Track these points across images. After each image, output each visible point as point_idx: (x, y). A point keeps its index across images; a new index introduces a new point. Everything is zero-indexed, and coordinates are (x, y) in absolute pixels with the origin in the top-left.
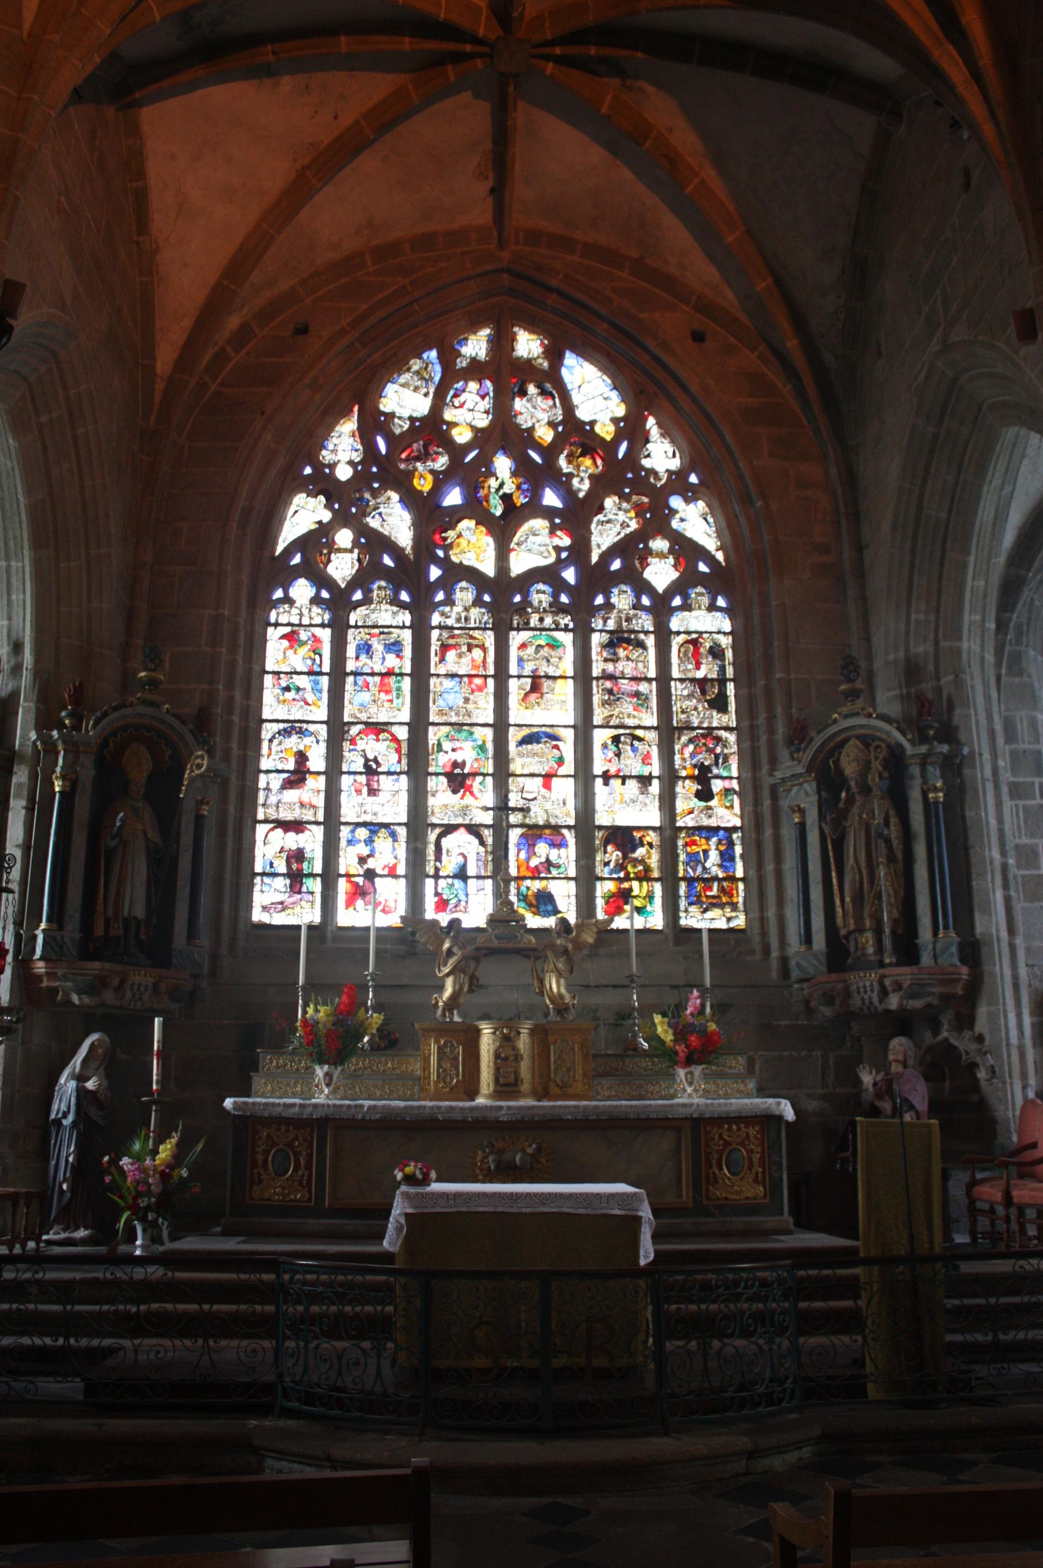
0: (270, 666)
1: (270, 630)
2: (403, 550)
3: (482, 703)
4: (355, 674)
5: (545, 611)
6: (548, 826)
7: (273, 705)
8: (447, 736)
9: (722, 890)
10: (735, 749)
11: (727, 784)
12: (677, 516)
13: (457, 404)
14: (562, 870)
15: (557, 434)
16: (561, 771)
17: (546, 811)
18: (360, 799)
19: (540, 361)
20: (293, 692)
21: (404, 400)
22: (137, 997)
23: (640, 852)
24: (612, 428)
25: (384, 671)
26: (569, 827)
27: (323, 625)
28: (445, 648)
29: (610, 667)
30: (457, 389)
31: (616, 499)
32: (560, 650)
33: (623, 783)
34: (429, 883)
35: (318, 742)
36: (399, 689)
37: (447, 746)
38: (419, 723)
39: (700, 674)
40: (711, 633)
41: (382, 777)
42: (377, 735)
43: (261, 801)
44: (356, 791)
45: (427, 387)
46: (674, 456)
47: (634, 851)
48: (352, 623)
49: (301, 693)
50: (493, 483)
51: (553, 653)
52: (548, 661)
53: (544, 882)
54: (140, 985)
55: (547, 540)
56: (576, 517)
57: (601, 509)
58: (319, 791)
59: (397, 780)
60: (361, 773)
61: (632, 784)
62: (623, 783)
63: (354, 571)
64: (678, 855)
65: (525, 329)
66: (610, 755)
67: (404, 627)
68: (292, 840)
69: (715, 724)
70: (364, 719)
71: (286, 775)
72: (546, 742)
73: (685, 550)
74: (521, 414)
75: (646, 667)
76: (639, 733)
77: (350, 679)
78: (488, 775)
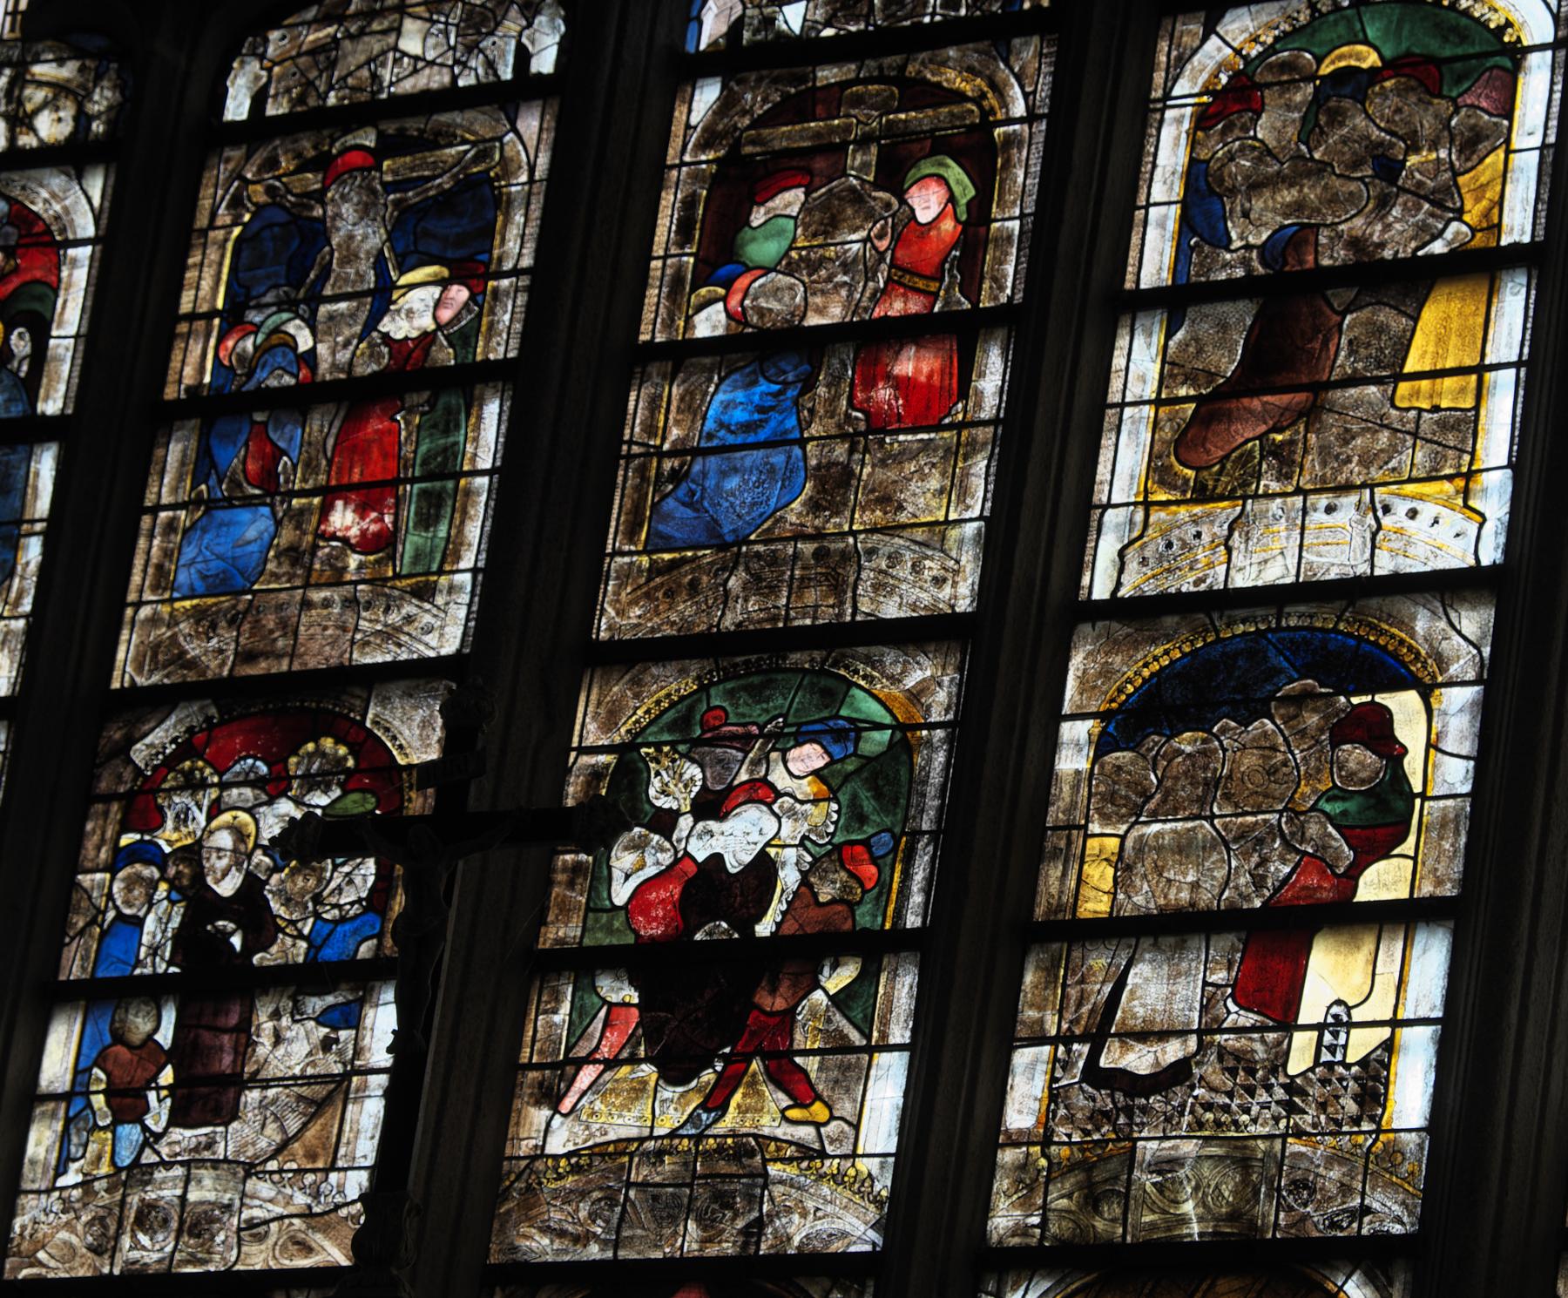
3: (923, 497)
4: (217, 407)
8: (681, 724)
16: (1383, 882)
17: (1240, 1157)
25: (365, 369)
36: (446, 469)
37: (675, 784)
48: (237, 107)
59: (349, 1016)
60: (153, 991)
72: (1301, 700)
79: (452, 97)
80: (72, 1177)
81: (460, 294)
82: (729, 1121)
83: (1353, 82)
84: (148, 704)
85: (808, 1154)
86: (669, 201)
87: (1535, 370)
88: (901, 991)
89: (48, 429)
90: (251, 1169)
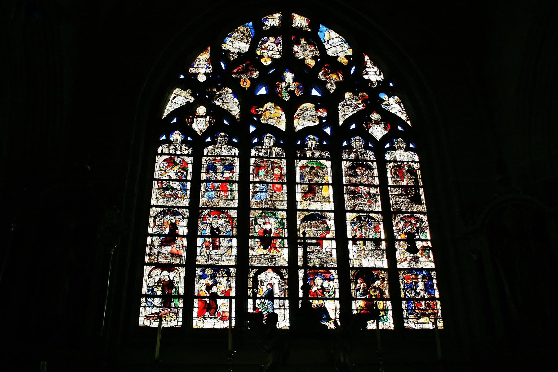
0: (156, 176)
1: (158, 157)
2: (234, 117)
3: (280, 198)
4: (206, 181)
5: (315, 149)
6: (321, 267)
7: (157, 198)
8: (260, 216)
9: (428, 305)
10: (427, 224)
11: (425, 244)
12: (384, 103)
13: (263, 47)
14: (331, 294)
15: (317, 63)
16: (328, 236)
18: (208, 251)
19: (307, 29)
20: (169, 191)
21: (236, 44)
23: (378, 283)
24: (346, 61)
26: (334, 269)
27: (188, 155)
28: (258, 168)
29: (353, 180)
30: (263, 40)
31: (351, 94)
32: (324, 170)
33: (365, 243)
34: (250, 302)
35: (183, 218)
36: (232, 191)
37: (260, 221)
38: (244, 208)
39: (404, 183)
40: (408, 162)
41: (221, 239)
42: (219, 215)
43: (148, 251)
44: (205, 247)
45: (247, 39)
46: (380, 74)
47: (374, 283)
48: (205, 153)
50: (283, 84)
51: (320, 171)
52: (318, 176)
53: (321, 301)
55: (314, 114)
56: (329, 102)
57: (344, 98)
58: (183, 247)
59: (231, 240)
60: (209, 237)
61: (369, 243)
62: (365, 243)
63: (207, 127)
64: (399, 285)
65: (299, 14)
66: (356, 227)
67: (234, 156)
69: (415, 210)
70: (211, 206)
71: (163, 238)
73: (389, 119)
74: (298, 53)
75: (373, 179)
76: (372, 215)
77: (203, 184)
78: (285, 238)
79: (227, 156)
80: (202, 254)
81: (231, 174)
82: (270, 254)
83: (314, 168)
84: (203, 209)
85: (279, 257)
86: (252, 168)
87: (334, 193)
88: (286, 241)
89: (189, 181)
90: (222, 255)
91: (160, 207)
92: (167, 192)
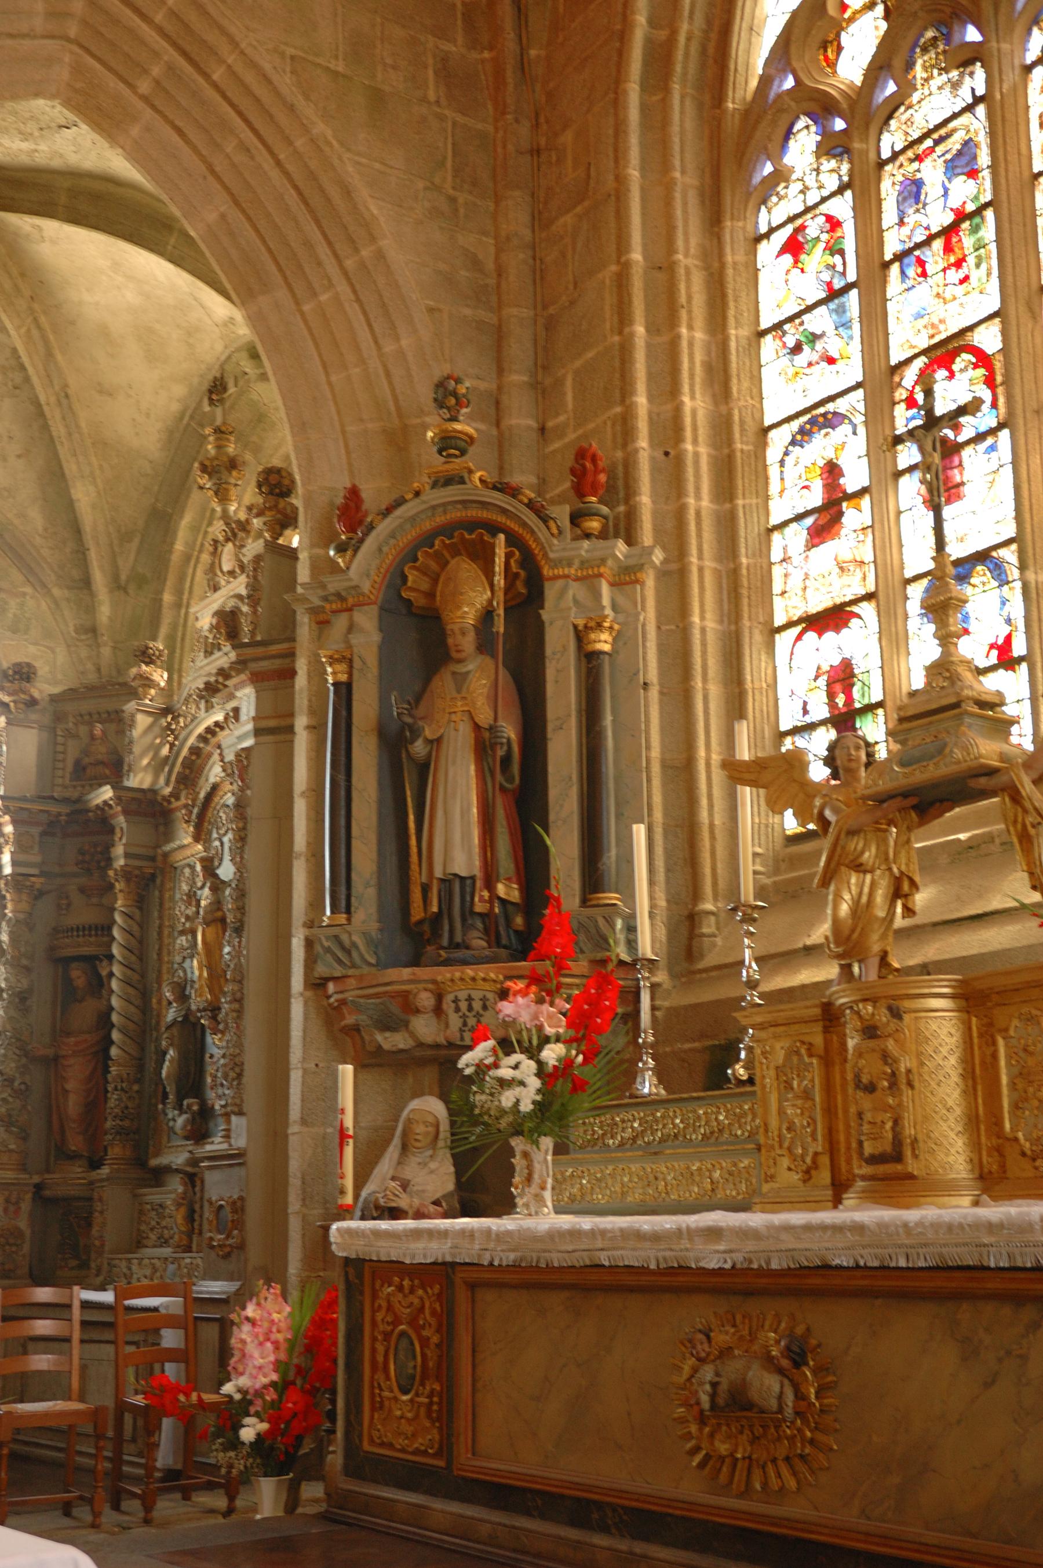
22: (472, 1022)
49: (819, 346)
54: (470, 999)
59: (993, 448)
68: (826, 649)
91: (788, 420)
92: (802, 359)
